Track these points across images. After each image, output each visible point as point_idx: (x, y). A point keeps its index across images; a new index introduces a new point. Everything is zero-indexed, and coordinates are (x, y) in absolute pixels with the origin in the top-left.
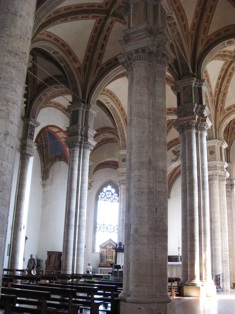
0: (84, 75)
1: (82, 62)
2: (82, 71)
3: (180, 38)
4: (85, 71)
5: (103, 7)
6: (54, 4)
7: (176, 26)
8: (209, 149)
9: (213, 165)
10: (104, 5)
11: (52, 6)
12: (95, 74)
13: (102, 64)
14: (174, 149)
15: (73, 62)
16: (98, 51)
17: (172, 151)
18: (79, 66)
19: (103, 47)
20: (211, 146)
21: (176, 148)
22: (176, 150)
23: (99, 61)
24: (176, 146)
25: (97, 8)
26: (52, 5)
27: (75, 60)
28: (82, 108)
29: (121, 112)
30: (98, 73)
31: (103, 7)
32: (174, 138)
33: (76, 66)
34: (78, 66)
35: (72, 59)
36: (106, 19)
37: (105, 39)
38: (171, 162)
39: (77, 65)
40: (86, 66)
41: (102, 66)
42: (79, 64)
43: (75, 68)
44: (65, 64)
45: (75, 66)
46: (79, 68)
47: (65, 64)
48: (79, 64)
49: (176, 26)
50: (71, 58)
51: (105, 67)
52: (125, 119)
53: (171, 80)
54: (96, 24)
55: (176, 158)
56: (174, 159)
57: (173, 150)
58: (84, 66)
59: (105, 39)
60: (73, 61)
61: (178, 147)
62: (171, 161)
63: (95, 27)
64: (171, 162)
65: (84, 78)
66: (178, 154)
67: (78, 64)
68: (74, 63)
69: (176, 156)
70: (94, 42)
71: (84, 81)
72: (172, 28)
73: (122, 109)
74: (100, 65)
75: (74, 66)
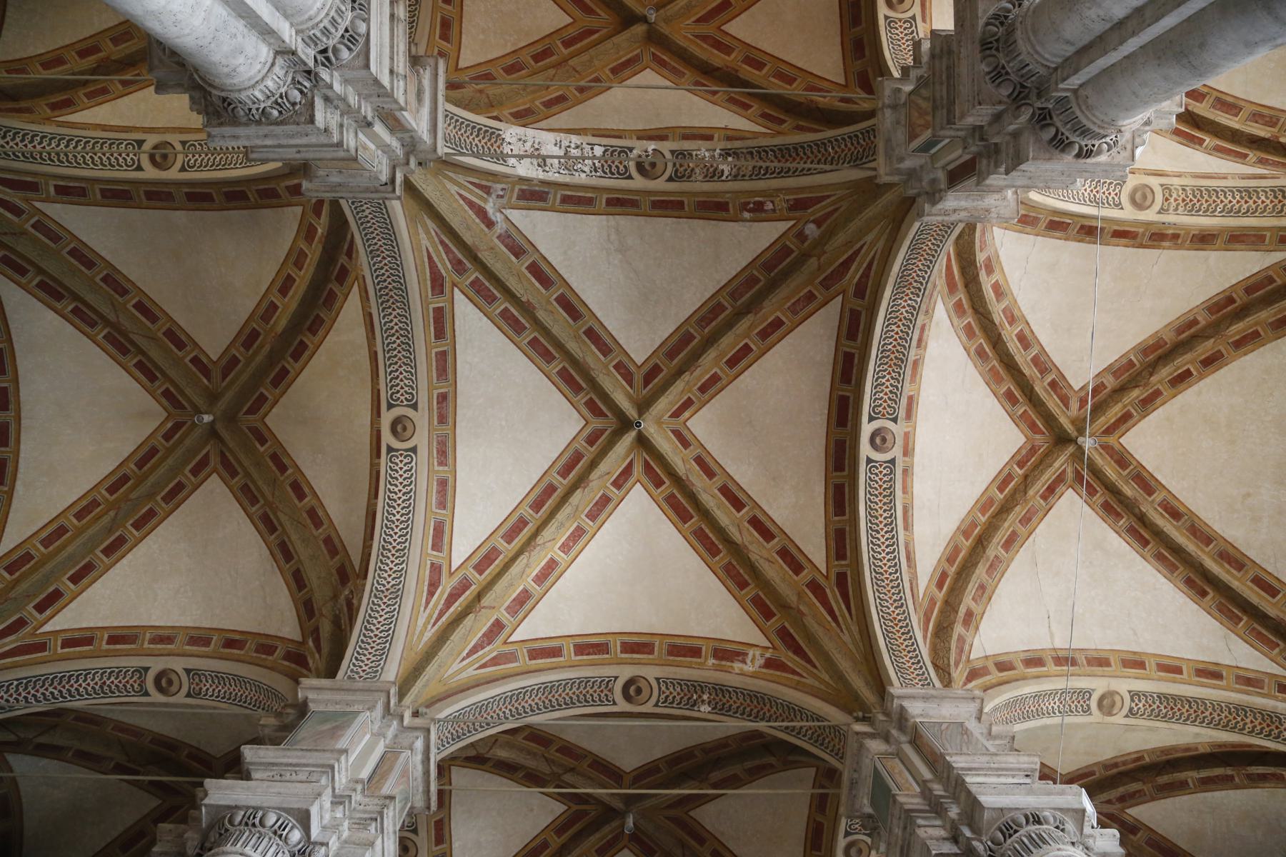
0: (809, 661)
1: (755, 636)
2: (788, 657)
3: (751, 153)
4: (798, 651)
5: (602, 432)
6: (403, 519)
7: (694, 153)
10: (597, 423)
11: (402, 526)
12: (840, 619)
13: (824, 571)
15: (729, 664)
16: (760, 552)
18: (762, 656)
19: (762, 527)
23: (806, 575)
25: (592, 449)
26: (397, 526)
27: (727, 653)
28: (875, 746)
29: (1224, 683)
30: (843, 607)
31: (602, 432)
33: (753, 663)
34: (760, 661)
35: (714, 661)
36: (643, 442)
37: (738, 504)
39: (752, 661)
40: (784, 634)
41: (833, 578)
42: (758, 652)
43: (754, 676)
44: (705, 697)
45: (748, 668)
46: (769, 664)
47: (705, 697)
48: (758, 652)
49: (691, 155)
50: (711, 661)
51: (843, 562)
53: (1139, 374)
54: (656, 492)
58: (778, 642)
59: (738, 504)
60: (724, 663)
63: (666, 507)
65: (815, 666)
67: (750, 656)
68: (737, 666)
70: (720, 547)
71: (827, 678)
72: (697, 171)
73: (1210, 673)
74: (822, 581)
75: (744, 675)
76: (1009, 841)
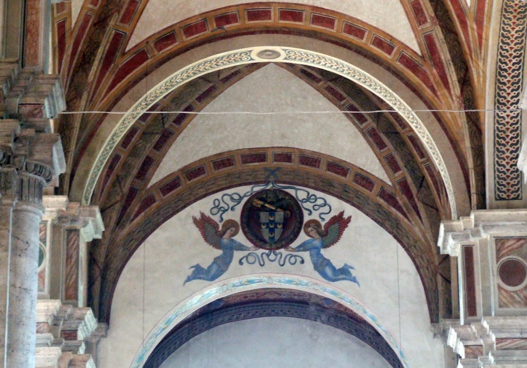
8: (498, 251)
9: (518, 335)
14: (207, 213)
17: (195, 221)
20: (508, 239)
21: (218, 208)
22: (216, 218)
24: (218, 195)
32: (212, 152)
38: (189, 279)
52: (62, 26)
55: (216, 260)
56: (205, 266)
57: (198, 216)
61: (231, 204)
62: (190, 272)
64: (189, 279)
66: (225, 240)
69: (219, 252)
76: (31, 175)
